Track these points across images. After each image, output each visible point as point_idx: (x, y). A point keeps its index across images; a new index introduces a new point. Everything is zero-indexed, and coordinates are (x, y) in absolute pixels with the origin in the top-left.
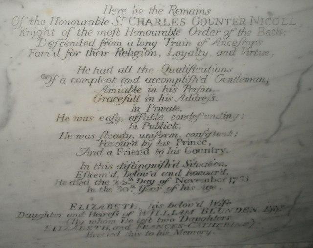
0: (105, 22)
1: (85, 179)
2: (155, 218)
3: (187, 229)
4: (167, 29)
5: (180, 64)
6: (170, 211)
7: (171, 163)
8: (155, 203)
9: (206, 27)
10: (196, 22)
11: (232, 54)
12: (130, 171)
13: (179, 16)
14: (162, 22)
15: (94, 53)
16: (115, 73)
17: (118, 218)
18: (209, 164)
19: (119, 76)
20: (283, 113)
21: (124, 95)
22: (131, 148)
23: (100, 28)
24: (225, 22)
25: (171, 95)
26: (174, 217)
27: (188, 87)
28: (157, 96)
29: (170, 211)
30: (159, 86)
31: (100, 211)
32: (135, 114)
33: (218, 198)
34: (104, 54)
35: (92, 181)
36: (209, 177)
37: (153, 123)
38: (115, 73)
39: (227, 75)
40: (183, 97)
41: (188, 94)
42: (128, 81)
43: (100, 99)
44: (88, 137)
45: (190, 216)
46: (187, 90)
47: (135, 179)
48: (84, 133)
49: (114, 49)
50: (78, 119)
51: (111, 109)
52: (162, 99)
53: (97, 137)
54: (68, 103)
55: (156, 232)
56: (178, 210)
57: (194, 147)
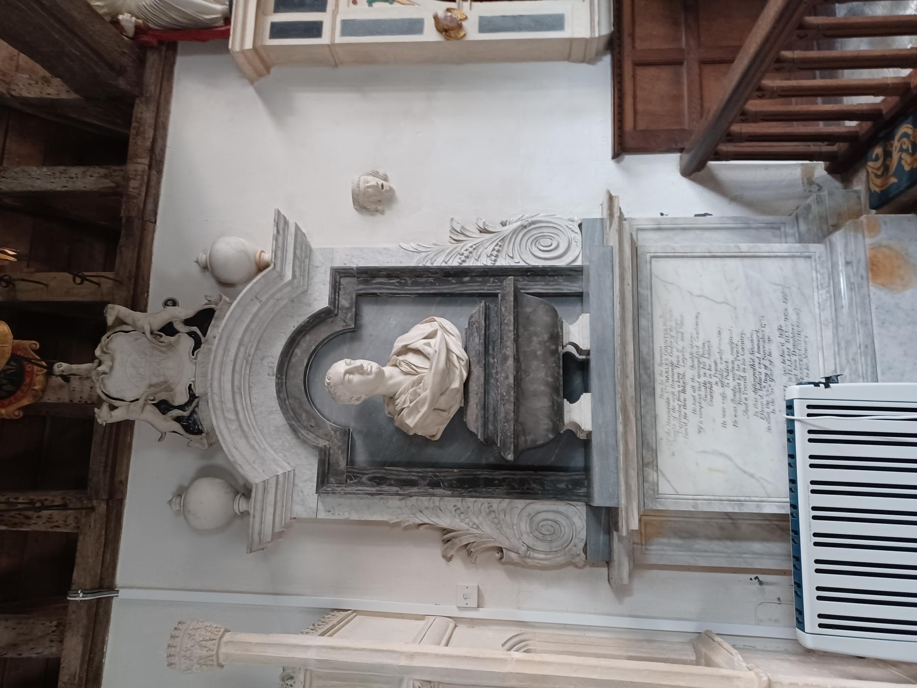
0: (668, 399)
2: (794, 372)
3: (803, 352)
4: (670, 368)
6: (789, 363)
7: (752, 363)
8: (783, 372)
9: (669, 348)
10: (666, 353)
11: (682, 334)
12: (758, 387)
13: (664, 361)
14: (667, 370)
15: (685, 405)
16: (694, 394)
18: (752, 341)
19: (697, 392)
21: (708, 390)
22: (742, 387)
23: (671, 401)
24: (666, 339)
25: (707, 364)
27: (702, 356)
28: (708, 372)
30: (702, 371)
32: (720, 384)
33: (777, 333)
35: (766, 410)
36: (761, 341)
37: (725, 374)
39: (695, 335)
40: (708, 358)
41: (707, 356)
42: (700, 387)
43: (711, 403)
45: (792, 350)
46: (704, 356)
47: (764, 384)
48: (733, 413)
49: (682, 394)
50: (724, 416)
51: (717, 398)
52: (710, 370)
53: (736, 406)
54: (714, 420)
55: (806, 371)
56: (787, 357)
57: (740, 350)
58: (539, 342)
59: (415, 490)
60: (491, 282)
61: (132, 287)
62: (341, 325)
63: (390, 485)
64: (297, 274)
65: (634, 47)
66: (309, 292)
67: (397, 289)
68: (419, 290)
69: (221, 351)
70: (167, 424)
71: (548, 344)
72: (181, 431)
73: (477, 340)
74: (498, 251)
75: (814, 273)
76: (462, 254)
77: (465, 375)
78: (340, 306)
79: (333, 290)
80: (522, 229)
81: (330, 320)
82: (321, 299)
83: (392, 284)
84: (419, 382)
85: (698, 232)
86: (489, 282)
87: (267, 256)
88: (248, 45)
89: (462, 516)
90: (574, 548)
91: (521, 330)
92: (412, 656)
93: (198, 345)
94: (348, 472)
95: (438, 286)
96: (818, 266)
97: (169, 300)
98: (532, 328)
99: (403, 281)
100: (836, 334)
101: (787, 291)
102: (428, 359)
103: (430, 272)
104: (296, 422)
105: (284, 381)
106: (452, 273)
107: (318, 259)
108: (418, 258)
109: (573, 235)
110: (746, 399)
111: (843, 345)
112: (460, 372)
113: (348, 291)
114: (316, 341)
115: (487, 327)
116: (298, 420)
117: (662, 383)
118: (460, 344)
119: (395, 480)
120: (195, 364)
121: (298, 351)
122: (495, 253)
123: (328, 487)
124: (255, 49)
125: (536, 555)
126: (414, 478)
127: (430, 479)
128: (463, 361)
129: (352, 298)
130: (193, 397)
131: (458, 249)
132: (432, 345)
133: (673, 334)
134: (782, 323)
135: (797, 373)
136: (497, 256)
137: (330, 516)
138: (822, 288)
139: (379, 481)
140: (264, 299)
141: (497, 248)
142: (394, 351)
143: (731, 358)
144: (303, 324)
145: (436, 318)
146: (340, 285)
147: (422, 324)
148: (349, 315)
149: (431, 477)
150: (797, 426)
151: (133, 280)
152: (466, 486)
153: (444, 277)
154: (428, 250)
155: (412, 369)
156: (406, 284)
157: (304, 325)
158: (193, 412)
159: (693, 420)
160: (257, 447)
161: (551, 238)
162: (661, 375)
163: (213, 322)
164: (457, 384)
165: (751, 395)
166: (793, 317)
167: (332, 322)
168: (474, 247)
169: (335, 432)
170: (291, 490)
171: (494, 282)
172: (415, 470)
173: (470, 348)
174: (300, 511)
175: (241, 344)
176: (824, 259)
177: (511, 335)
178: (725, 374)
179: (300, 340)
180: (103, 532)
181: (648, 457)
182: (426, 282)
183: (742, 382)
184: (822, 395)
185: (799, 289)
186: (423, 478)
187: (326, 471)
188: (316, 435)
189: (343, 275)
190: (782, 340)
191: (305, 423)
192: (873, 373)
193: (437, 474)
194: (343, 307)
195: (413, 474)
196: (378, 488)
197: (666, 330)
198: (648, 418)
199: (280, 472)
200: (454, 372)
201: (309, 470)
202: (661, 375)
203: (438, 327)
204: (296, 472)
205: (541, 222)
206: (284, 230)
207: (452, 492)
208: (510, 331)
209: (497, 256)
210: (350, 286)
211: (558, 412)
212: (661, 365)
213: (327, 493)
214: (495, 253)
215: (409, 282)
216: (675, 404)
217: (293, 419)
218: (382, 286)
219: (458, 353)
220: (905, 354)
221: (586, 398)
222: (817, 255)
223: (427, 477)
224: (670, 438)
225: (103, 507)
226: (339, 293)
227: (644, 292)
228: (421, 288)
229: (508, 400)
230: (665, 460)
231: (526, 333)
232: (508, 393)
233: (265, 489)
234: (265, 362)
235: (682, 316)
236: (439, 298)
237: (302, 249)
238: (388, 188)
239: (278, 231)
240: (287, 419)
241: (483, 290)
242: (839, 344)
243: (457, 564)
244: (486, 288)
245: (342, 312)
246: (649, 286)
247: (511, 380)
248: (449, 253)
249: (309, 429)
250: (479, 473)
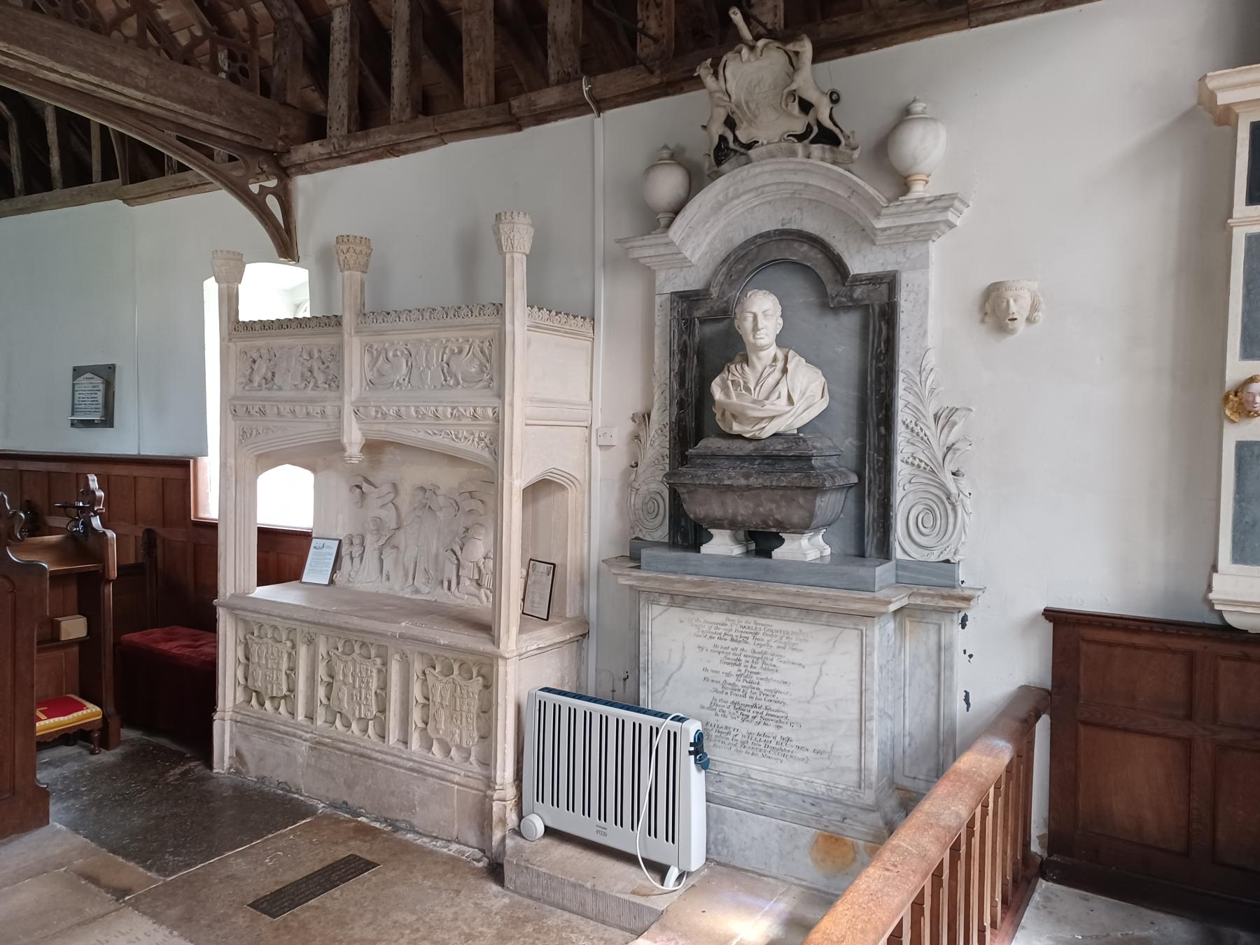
0: (726, 625)
1: (714, 707)
5: (760, 650)
6: (758, 739)
11: (784, 648)
15: (721, 639)
16: (730, 650)
17: (730, 737)
18: (778, 711)
20: (815, 686)
22: (737, 692)
23: (724, 627)
26: (760, 743)
27: (764, 662)
28: (749, 665)
29: (758, 738)
30: (750, 660)
31: (721, 730)
32: (739, 673)
34: (726, 640)
35: (718, 709)
38: (730, 650)
39: (782, 659)
41: (764, 666)
44: (717, 682)
47: (740, 712)
49: (730, 638)
50: (713, 671)
51: (728, 669)
52: (751, 667)
54: (708, 662)
55: (751, 752)
56: (763, 739)
58: (771, 510)
59: (676, 387)
61: (877, 31)
63: (680, 362)
64: (888, 232)
65: (1224, 658)
66: (874, 248)
69: (791, 166)
70: (718, 129)
71: (771, 518)
72: (714, 147)
73: (779, 447)
74: (919, 466)
75: (844, 787)
76: (916, 425)
80: (947, 495)
81: (839, 278)
82: (860, 263)
83: (879, 345)
84: (748, 389)
85: (935, 691)
86: (879, 455)
87: (919, 190)
88: (1223, 99)
89: (659, 431)
90: (638, 529)
91: (781, 492)
92: (512, 405)
93: (800, 138)
96: (849, 792)
97: (838, 95)
98: (784, 504)
99: (882, 358)
100: (781, 788)
101: (826, 756)
105: (774, 239)
107: (915, 251)
108: (913, 372)
109: (936, 553)
110: (726, 693)
111: (770, 791)
112: (748, 431)
113: (872, 294)
115: (788, 458)
116: (736, 262)
117: (739, 621)
118: (781, 429)
119: (685, 366)
120: (780, 140)
121: (805, 248)
122: (917, 462)
123: (678, 303)
124: (1228, 108)
125: (633, 496)
129: (863, 300)
130: (750, 146)
131: (923, 420)
132: (777, 402)
133: (784, 639)
134: (794, 743)
135: (750, 744)
136: (913, 464)
137: (657, 307)
138: (827, 790)
139: (683, 351)
140: (852, 200)
141: (923, 465)
143: (762, 688)
148: (844, 300)
150: (662, 720)
151: (885, 30)
152: (681, 435)
154: (923, 384)
156: (878, 360)
158: (736, 152)
159: (709, 644)
160: (708, 225)
161: (934, 526)
162: (746, 622)
163: (827, 147)
164: (736, 428)
165: (731, 698)
166: (800, 754)
167: (836, 281)
168: (925, 438)
169: (726, 302)
171: (878, 461)
173: (774, 440)
174: (661, 276)
175: (807, 185)
176: (857, 800)
177: (768, 483)
178: (748, 680)
180: (637, 89)
181: (678, 599)
182: (880, 384)
183: (741, 693)
184: (684, 747)
185: (828, 768)
186: (686, 394)
190: (778, 739)
191: (734, 269)
192: (740, 806)
196: (676, 351)
197: (788, 633)
198: (709, 605)
199: (687, 254)
200: (749, 424)
201: (690, 281)
202: (746, 622)
205: (956, 517)
206: (934, 208)
208: (771, 482)
209: (907, 463)
210: (879, 295)
211: (719, 525)
212: (756, 623)
213: (672, 303)
214: (917, 462)
215: (881, 365)
216: (722, 630)
220: (754, 838)
221: (737, 551)
222: (862, 795)
223: (688, 397)
224: (694, 621)
225: (655, 81)
227: (825, 617)
228: (874, 378)
229: (709, 479)
230: (676, 614)
231: (778, 497)
232: (716, 479)
233: (667, 244)
234: (797, 212)
235: (801, 650)
237: (921, 231)
238: (1010, 327)
239: (929, 202)
240: (735, 251)
241: (870, 449)
242: (772, 788)
243: (629, 426)
244: (872, 452)
246: (831, 624)
247: (727, 482)
248: (918, 409)
249: (729, 274)
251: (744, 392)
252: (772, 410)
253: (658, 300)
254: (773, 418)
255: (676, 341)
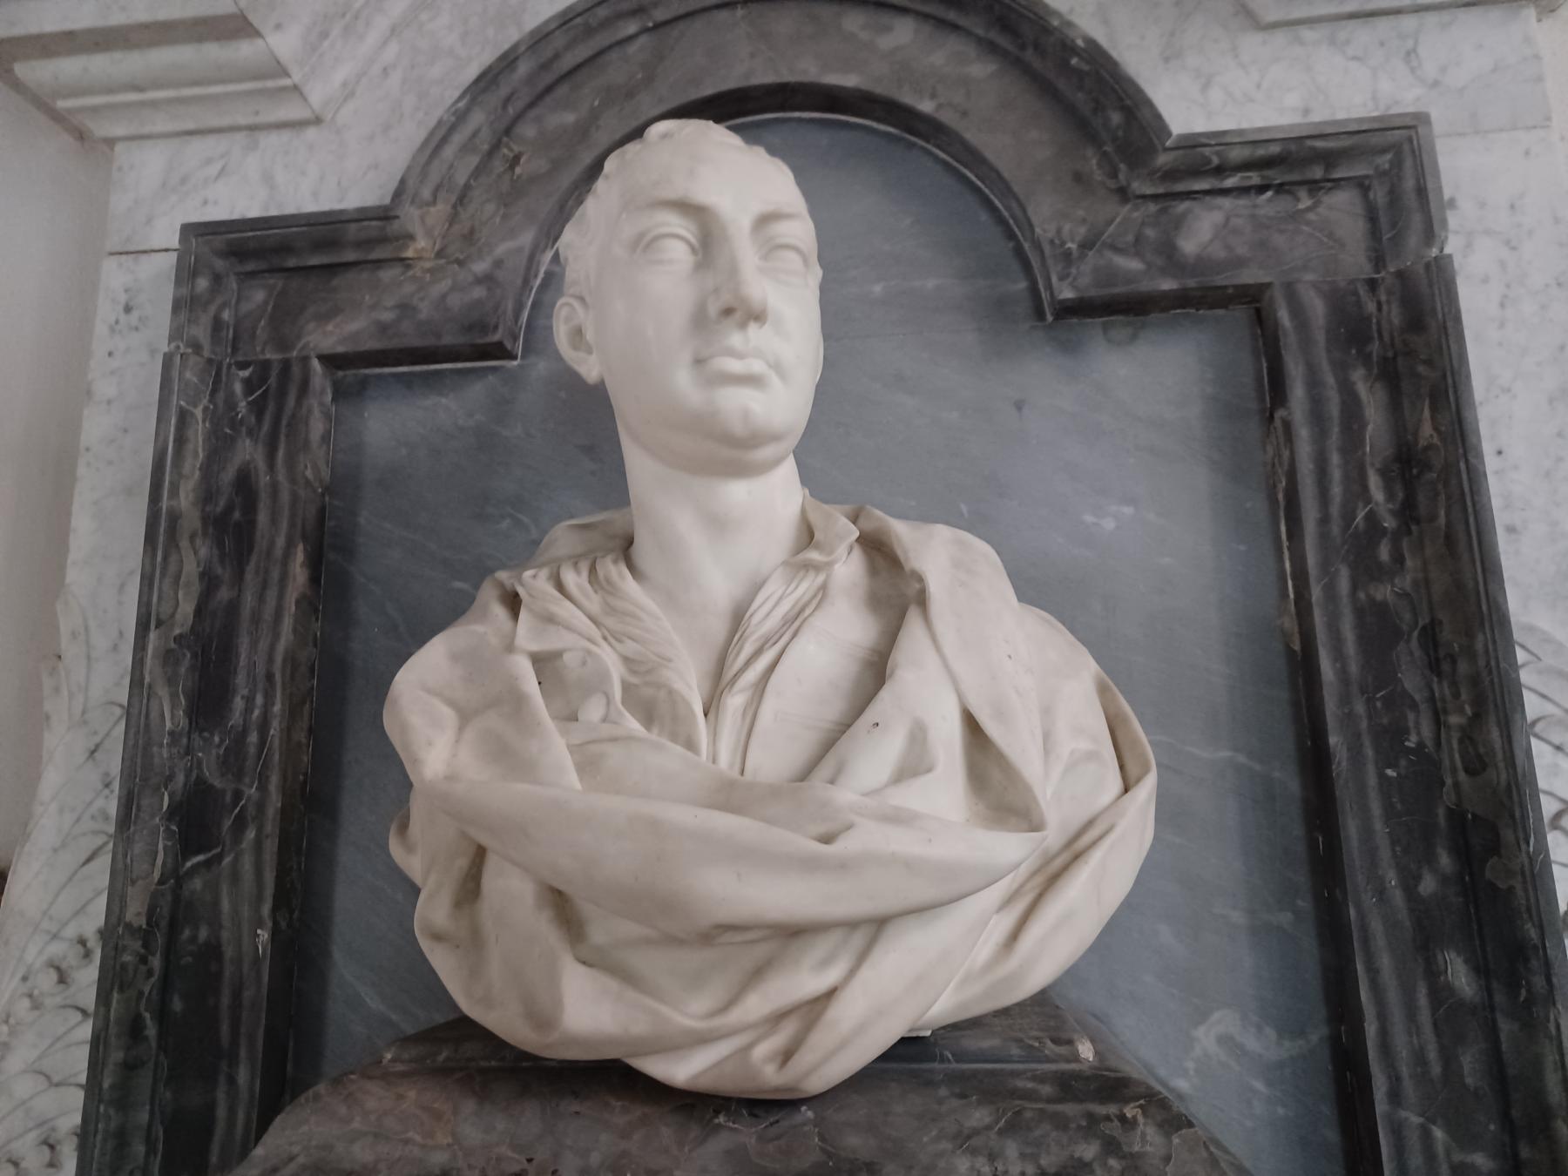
59: (170, 714)
60: (1458, 1157)
62: (1067, 228)
63: (209, 582)
66: (1252, 44)
67: (1324, 520)
68: (1338, 655)
77: (680, 1071)
78: (1183, 206)
79: (1275, 149)
81: (1092, 163)
86: (1464, 1137)
89: (47, 980)
94: (286, 366)
95: (1382, 776)
99: (1384, 553)
102: (805, 774)
103: (1477, 717)
104: (530, 79)
106: (1491, 871)
113: (1279, 240)
114: (965, 114)
119: (233, 608)
123: (217, 279)
126: (238, 704)
127: (228, 798)
128: (787, 1055)
129: (1240, 263)
132: (910, 797)
137: (106, 312)
142: (903, 532)
144: (1056, 23)
145: (1146, 789)
146: (1314, 186)
147: (1103, 690)
148: (1133, 265)
149: (238, 795)
152: (177, 1005)
153: (1457, 817)
155: (758, 652)
156: (1366, 570)
157: (1046, 30)
167: (1078, 178)
169: (487, 280)
170: (226, 121)
172: (277, 708)
179: (968, 33)
186: (233, 762)
187: (292, 262)
188: (467, 187)
189: (1379, 194)
193: (251, 834)
194: (1178, 223)
195: (259, 700)
196: (191, 519)
199: (283, 43)
203: (1058, 819)
204: (311, 133)
207: (143, 922)
215: (1383, 592)
217: (545, 67)
218: (1335, 431)
219: (846, 1012)
223: (239, 776)
226: (1261, 189)
228: (1354, 668)
236: (1289, 781)
240: (540, 37)
241: (1395, 1096)
245: (1143, 224)
250: (243, 1076)
251: (633, 725)
252: (910, 865)
253: (115, 277)
254: (878, 925)
255: (193, 464)
